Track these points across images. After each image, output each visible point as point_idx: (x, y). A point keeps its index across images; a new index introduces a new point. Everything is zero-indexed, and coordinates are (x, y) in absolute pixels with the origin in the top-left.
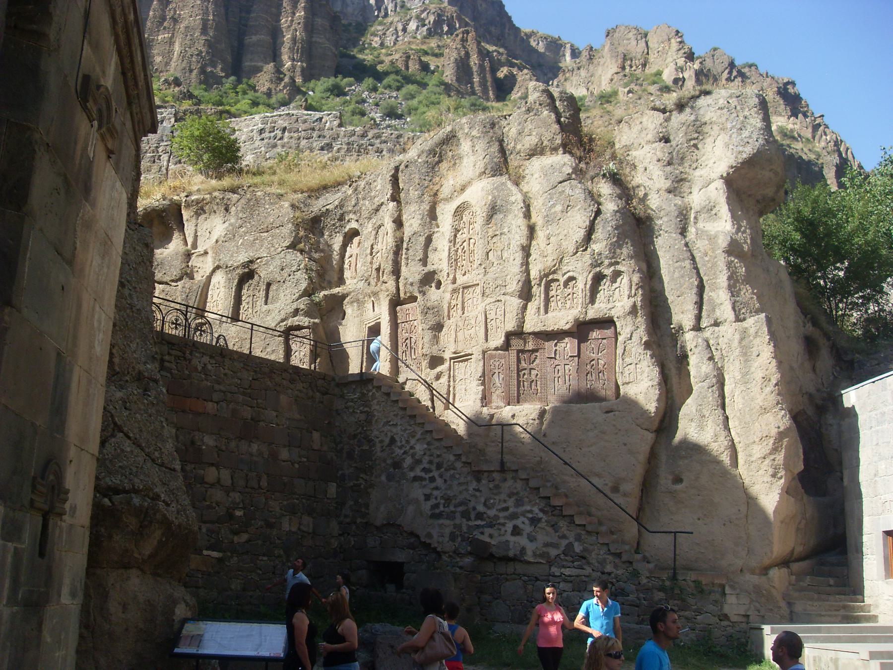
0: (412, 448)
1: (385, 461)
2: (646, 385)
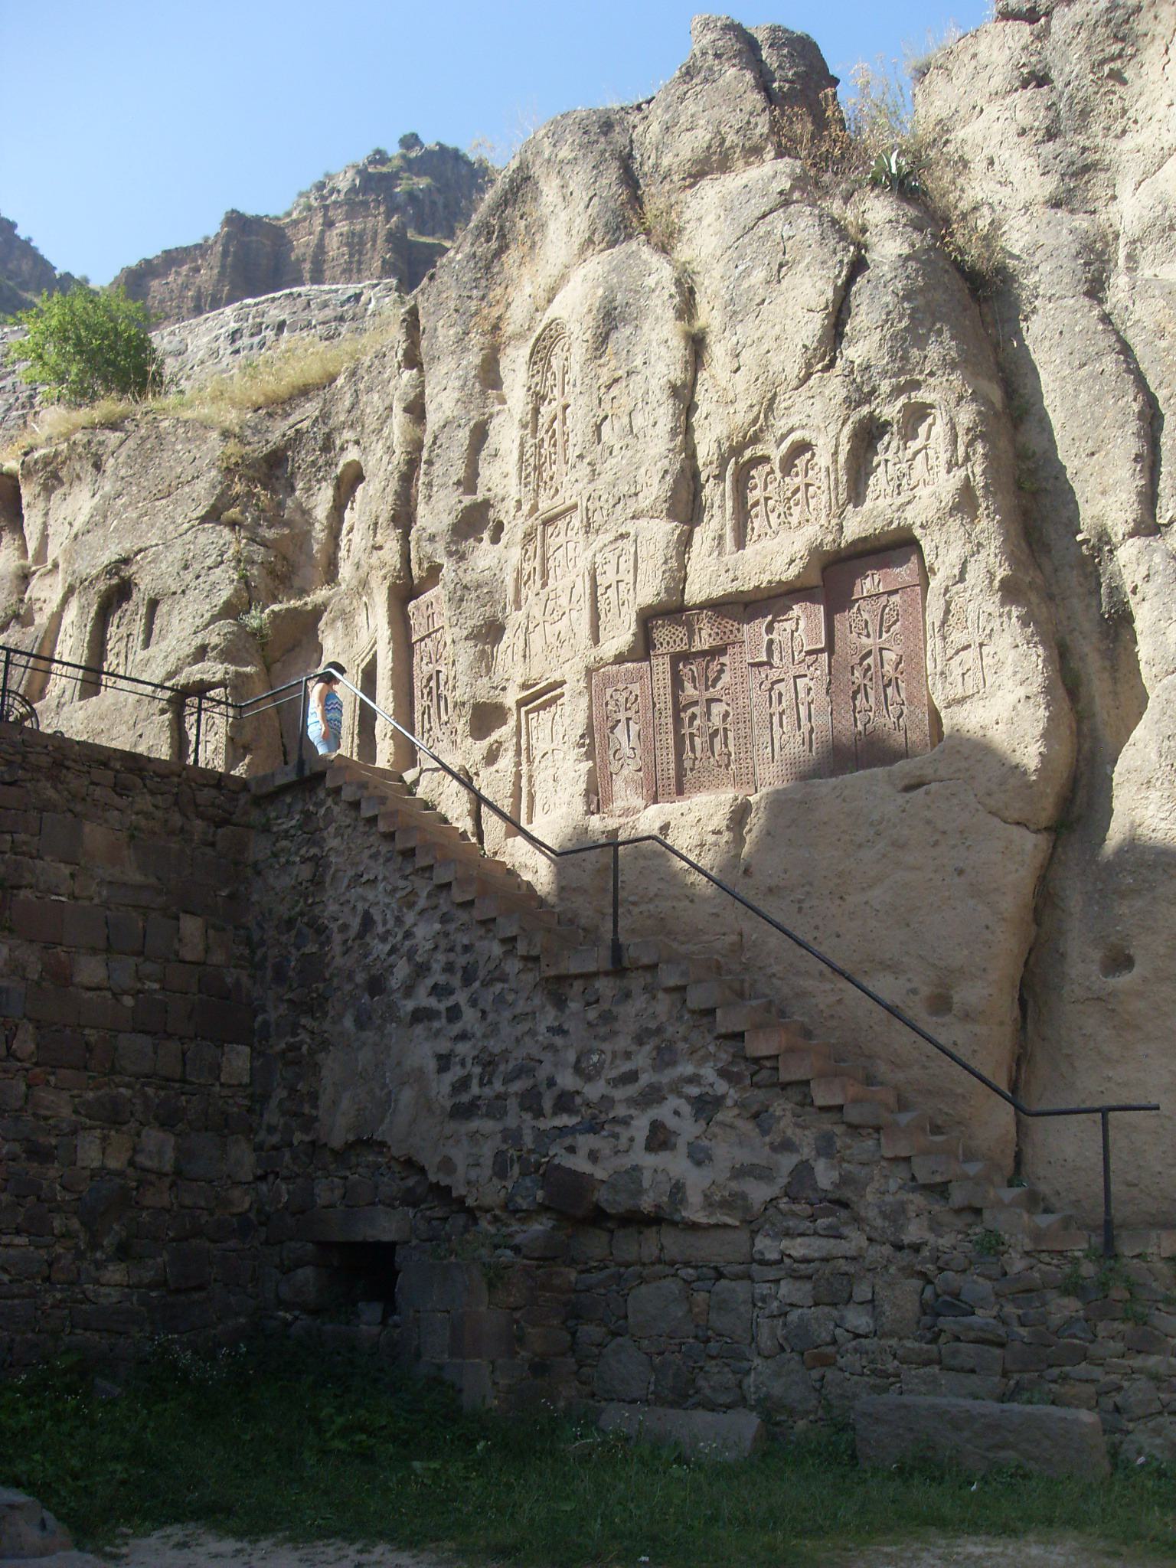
0: (408, 935)
1: (350, 977)
2: (1012, 699)
